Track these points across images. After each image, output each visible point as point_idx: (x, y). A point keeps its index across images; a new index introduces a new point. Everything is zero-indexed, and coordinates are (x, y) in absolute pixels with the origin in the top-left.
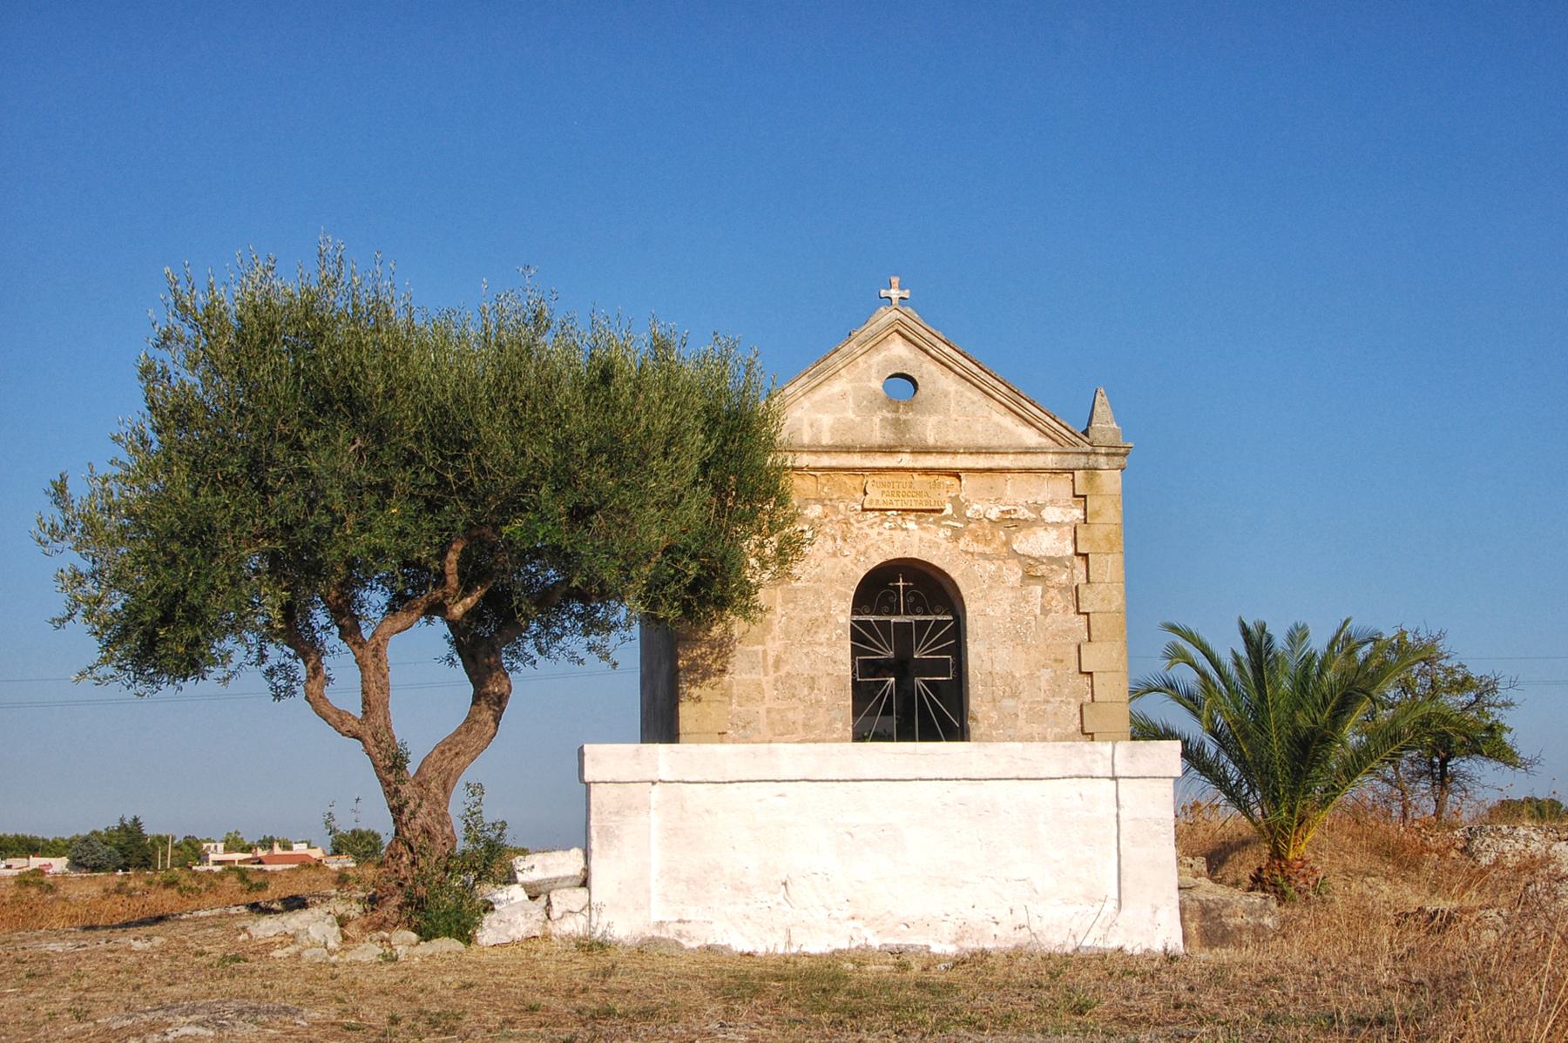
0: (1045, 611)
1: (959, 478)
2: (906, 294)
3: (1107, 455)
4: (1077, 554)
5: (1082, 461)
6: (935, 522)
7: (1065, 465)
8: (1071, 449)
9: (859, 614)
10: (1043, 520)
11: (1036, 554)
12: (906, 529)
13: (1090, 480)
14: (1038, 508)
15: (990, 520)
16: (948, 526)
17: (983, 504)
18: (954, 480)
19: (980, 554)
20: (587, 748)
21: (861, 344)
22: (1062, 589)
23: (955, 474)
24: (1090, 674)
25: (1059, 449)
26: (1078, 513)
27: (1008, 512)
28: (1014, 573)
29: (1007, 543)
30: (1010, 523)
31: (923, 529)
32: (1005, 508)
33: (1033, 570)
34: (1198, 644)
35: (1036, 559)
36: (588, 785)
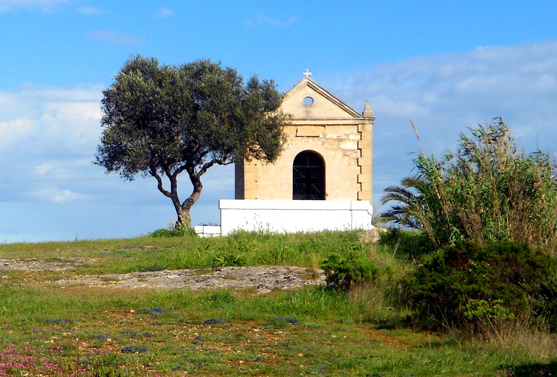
0: (349, 165)
1: (325, 127)
2: (310, 74)
3: (368, 120)
4: (358, 149)
5: (361, 122)
6: (317, 140)
7: (356, 123)
8: (357, 118)
9: (296, 165)
10: (349, 139)
11: (347, 149)
12: (309, 142)
13: (363, 128)
14: (347, 135)
15: (334, 139)
16: (321, 141)
17: (331, 133)
18: (324, 127)
19: (330, 149)
20: (221, 201)
21: (297, 89)
22: (354, 158)
23: (324, 126)
24: (361, 183)
25: (354, 118)
26: (359, 137)
27: (339, 136)
28: (340, 154)
29: (338, 146)
30: (340, 140)
31: (314, 141)
32: (338, 135)
33: (345, 153)
34: (212, 162)
35: (347, 150)
36: (221, 209)
